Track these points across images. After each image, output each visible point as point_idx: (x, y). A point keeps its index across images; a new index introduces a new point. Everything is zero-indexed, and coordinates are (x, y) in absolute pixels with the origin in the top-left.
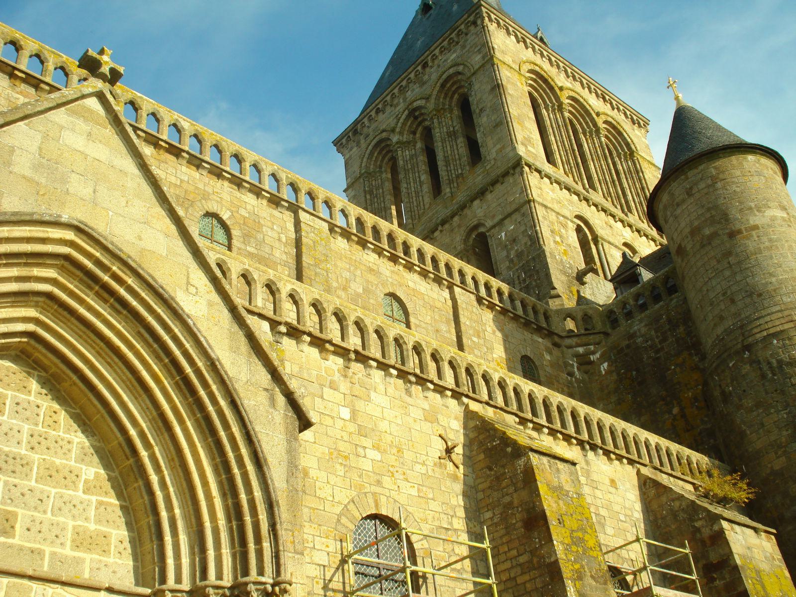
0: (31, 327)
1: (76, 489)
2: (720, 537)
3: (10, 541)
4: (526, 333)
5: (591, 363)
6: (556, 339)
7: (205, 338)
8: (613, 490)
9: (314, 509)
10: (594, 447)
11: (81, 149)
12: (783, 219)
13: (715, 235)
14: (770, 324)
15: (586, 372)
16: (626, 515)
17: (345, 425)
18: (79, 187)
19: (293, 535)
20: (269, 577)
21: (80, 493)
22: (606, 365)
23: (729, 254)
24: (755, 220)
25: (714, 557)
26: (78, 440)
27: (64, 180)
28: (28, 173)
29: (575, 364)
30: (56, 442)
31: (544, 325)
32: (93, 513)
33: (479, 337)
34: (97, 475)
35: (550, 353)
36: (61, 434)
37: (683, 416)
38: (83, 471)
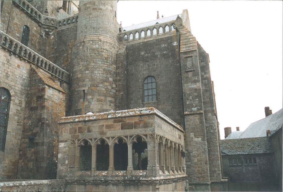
2: (43, 90)
4: (29, 19)
5: (49, 35)
6: (40, 24)
8: (17, 68)
10: (15, 54)
12: (110, 10)
13: (90, 7)
14: (92, 37)
15: (47, 37)
16: (19, 77)
22: (53, 36)
23: (91, 14)
24: (101, 7)
25: (40, 95)
29: (44, 34)
31: (38, 20)
33: (9, 14)
35: (37, 28)
37: (67, 57)
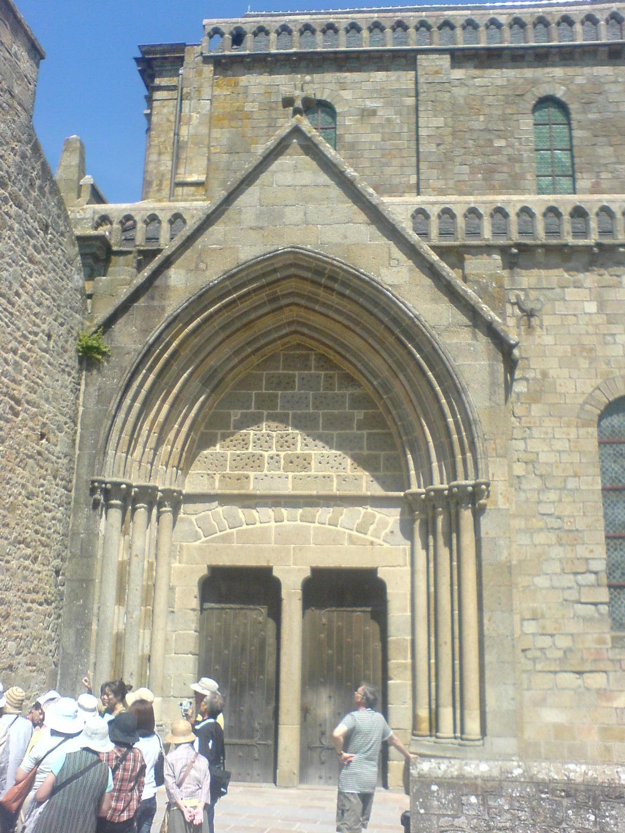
0: (293, 328)
1: (351, 428)
3: (309, 473)
7: (402, 303)
9: (554, 404)
11: (290, 184)
17: (590, 320)
18: (293, 215)
19: (495, 443)
20: (472, 480)
21: (355, 430)
26: (350, 392)
27: (281, 216)
28: (253, 224)
30: (333, 398)
32: (365, 443)
34: (366, 414)
36: (336, 392)
38: (356, 414)
